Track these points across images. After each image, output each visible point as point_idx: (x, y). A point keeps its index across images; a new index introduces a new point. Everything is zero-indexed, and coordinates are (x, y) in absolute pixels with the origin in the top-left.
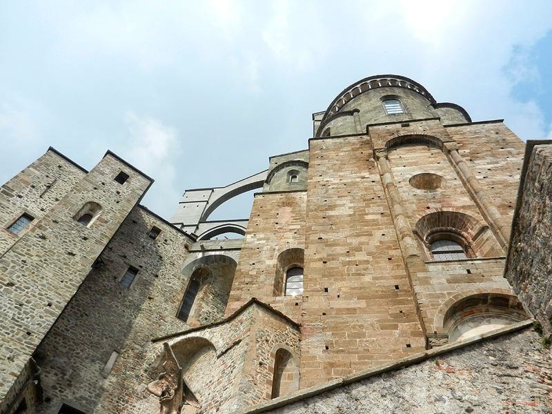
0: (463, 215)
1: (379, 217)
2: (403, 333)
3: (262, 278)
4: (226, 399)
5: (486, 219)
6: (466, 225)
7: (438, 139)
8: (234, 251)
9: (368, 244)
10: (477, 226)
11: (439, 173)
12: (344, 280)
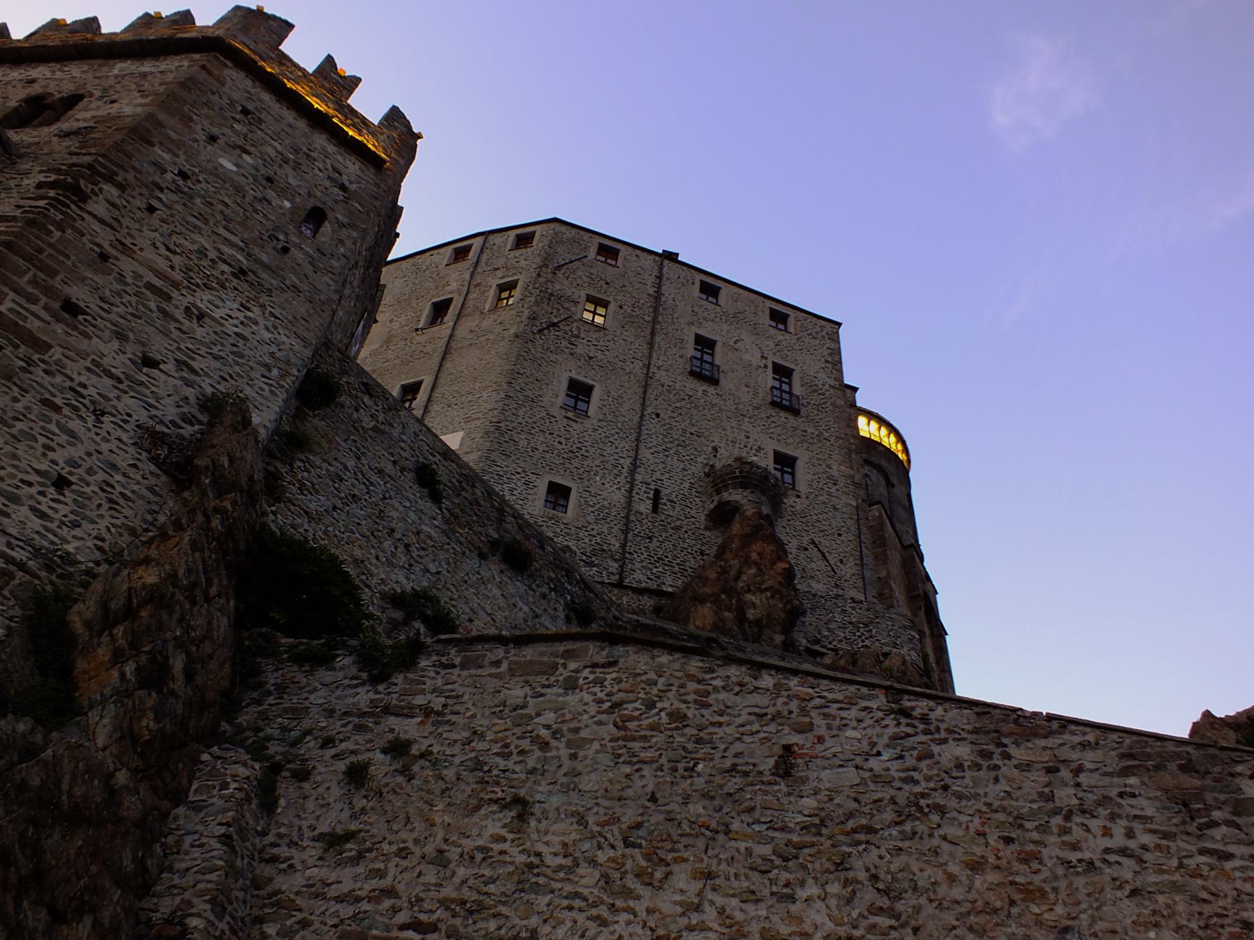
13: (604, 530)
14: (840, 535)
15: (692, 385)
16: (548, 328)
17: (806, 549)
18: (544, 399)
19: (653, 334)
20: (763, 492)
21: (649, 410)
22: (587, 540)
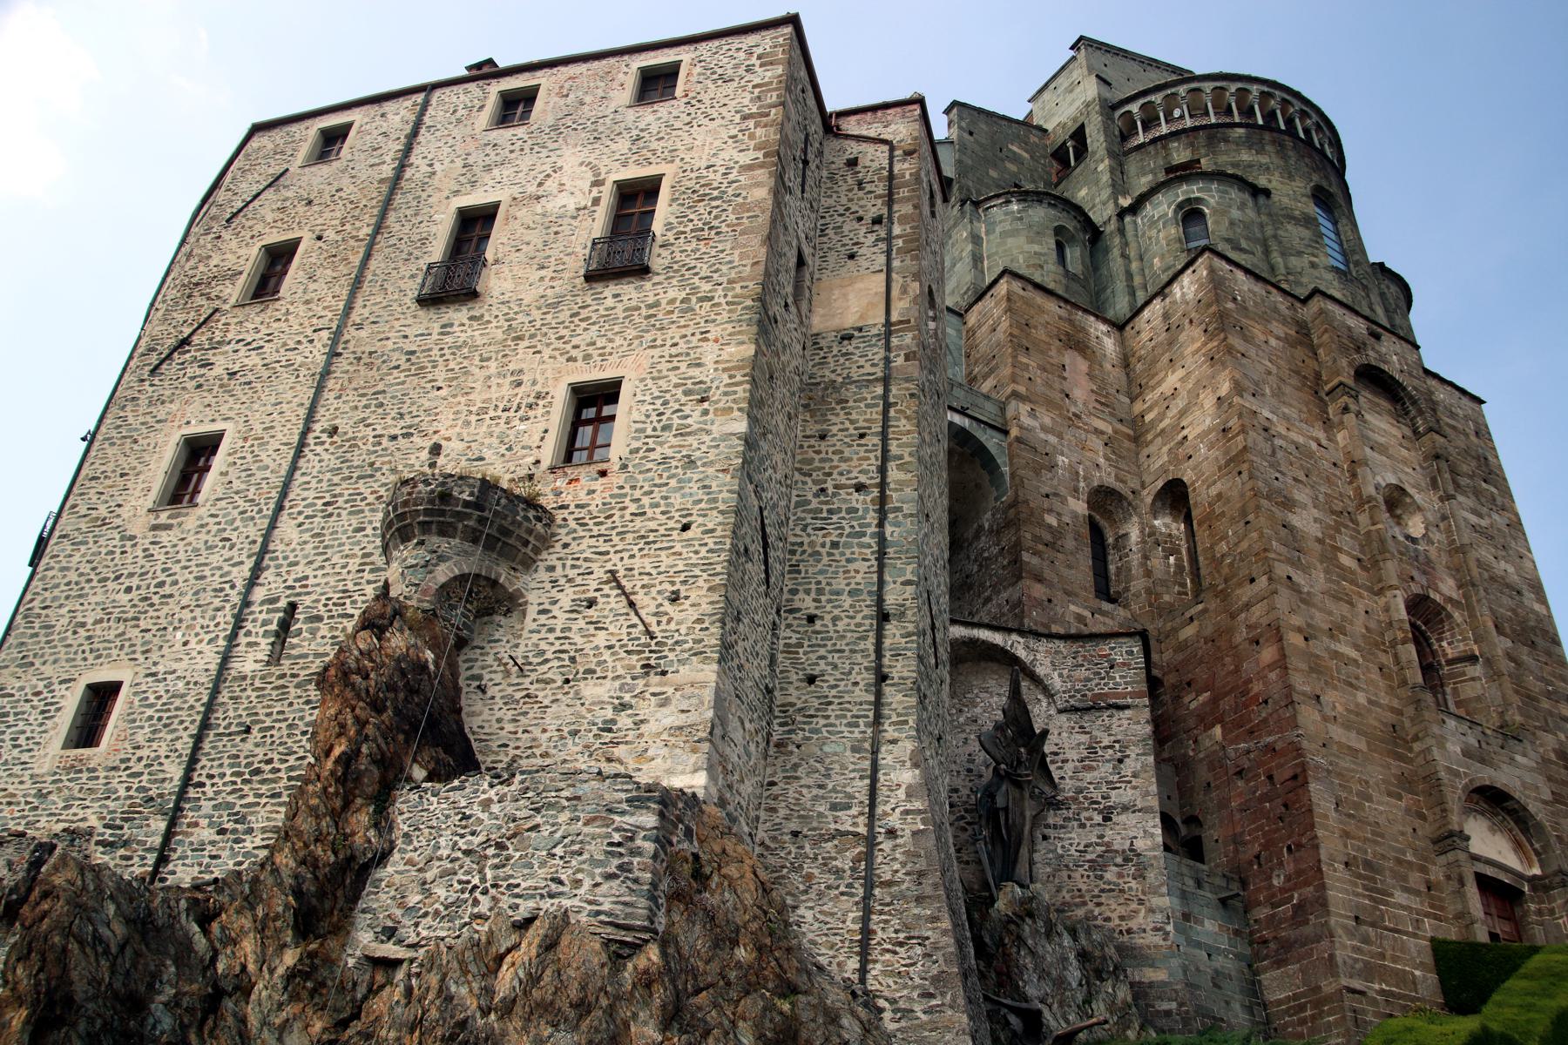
0: (1450, 616)
2: (1408, 811)
3: (1070, 543)
4: (1125, 808)
7: (1421, 412)
8: (989, 431)
9: (1351, 624)
11: (1417, 497)
12: (1335, 688)
13: (162, 752)
14: (686, 528)
15: (430, 321)
16: (169, 356)
17: (591, 603)
18: (125, 512)
19: (368, 256)
20: (444, 531)
21: (317, 427)
22: (122, 793)
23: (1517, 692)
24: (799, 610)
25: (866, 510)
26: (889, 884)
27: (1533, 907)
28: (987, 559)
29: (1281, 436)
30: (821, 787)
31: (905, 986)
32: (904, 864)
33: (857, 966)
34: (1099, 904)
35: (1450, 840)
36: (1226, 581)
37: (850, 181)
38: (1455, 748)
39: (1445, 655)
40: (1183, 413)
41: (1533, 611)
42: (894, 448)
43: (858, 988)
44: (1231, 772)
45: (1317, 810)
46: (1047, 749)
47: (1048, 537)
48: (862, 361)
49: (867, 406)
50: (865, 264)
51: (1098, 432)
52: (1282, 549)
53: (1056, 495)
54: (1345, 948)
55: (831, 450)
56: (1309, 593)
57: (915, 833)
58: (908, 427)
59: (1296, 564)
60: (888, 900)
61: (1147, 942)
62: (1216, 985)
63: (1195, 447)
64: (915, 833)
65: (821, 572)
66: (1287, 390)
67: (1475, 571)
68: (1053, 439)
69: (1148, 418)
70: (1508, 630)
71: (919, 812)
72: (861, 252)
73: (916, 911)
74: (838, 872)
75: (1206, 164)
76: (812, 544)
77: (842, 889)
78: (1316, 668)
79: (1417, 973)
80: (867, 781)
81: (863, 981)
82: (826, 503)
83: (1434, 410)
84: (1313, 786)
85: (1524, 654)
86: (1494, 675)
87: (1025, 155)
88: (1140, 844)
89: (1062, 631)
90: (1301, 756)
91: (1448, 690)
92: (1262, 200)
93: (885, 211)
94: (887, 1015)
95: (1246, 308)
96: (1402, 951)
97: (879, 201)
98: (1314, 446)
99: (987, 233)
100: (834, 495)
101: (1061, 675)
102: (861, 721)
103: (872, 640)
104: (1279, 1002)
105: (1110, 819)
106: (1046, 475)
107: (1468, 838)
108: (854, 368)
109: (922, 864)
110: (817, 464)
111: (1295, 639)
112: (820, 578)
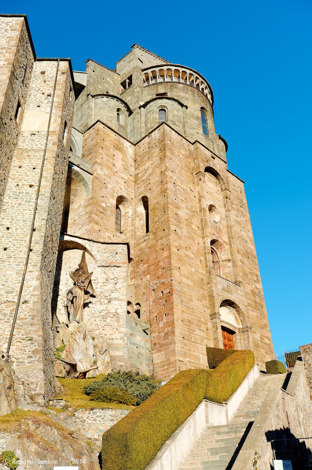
0: (224, 247)
1: (196, 228)
3: (109, 213)
4: (115, 299)
5: (232, 254)
6: (222, 252)
7: (224, 183)
9: (193, 247)
10: (227, 256)
11: (219, 209)
12: (185, 266)
23: (242, 272)
24: (4, 225)
25: (32, 194)
26: (22, 319)
27: (238, 337)
28: (81, 215)
29: (179, 186)
30: (3, 285)
31: (23, 354)
32: (28, 313)
33: (7, 347)
34: (103, 330)
35: (214, 315)
36: (156, 229)
37: (41, 80)
38: (220, 287)
39: (221, 259)
40: (150, 175)
41: (250, 248)
42: (44, 174)
43: (5, 355)
44: (151, 290)
45: (174, 303)
46: (92, 279)
47: (102, 210)
48: (38, 143)
49: (37, 159)
50: (43, 110)
51: (123, 178)
52: (175, 221)
53: (106, 197)
54: (178, 347)
55: (22, 172)
56: (181, 236)
57: (34, 302)
58: (50, 168)
59: (178, 226)
60: (21, 324)
61: (117, 342)
62: (138, 357)
63: (152, 187)
64: (34, 302)
65: (13, 213)
66: (183, 171)
67: (233, 234)
68: (107, 179)
69: (139, 176)
70: (241, 253)
71: (37, 295)
72: (42, 105)
73: (30, 328)
74: (5, 315)
75: (169, 95)
76: (11, 203)
77: (6, 320)
78: (180, 260)
79: (200, 356)
80: (20, 284)
81: (8, 352)
82: (19, 190)
83: (228, 183)
84: (174, 295)
85: (246, 261)
86: (235, 265)
87: (112, 82)
88: (118, 311)
89: (103, 241)
90: (171, 286)
91: (221, 269)
92: (184, 108)
93: (52, 92)
94: (15, 364)
95: (174, 144)
96: (197, 349)
97: (51, 89)
98: (189, 190)
99: (95, 107)
100: (22, 187)
101: (100, 255)
102: (21, 264)
103: (29, 237)
104: (158, 364)
105: (110, 302)
106: (104, 190)
107: (220, 315)
108: (35, 145)
109: (35, 313)
110: (17, 176)
111: (174, 250)
112: (13, 215)
